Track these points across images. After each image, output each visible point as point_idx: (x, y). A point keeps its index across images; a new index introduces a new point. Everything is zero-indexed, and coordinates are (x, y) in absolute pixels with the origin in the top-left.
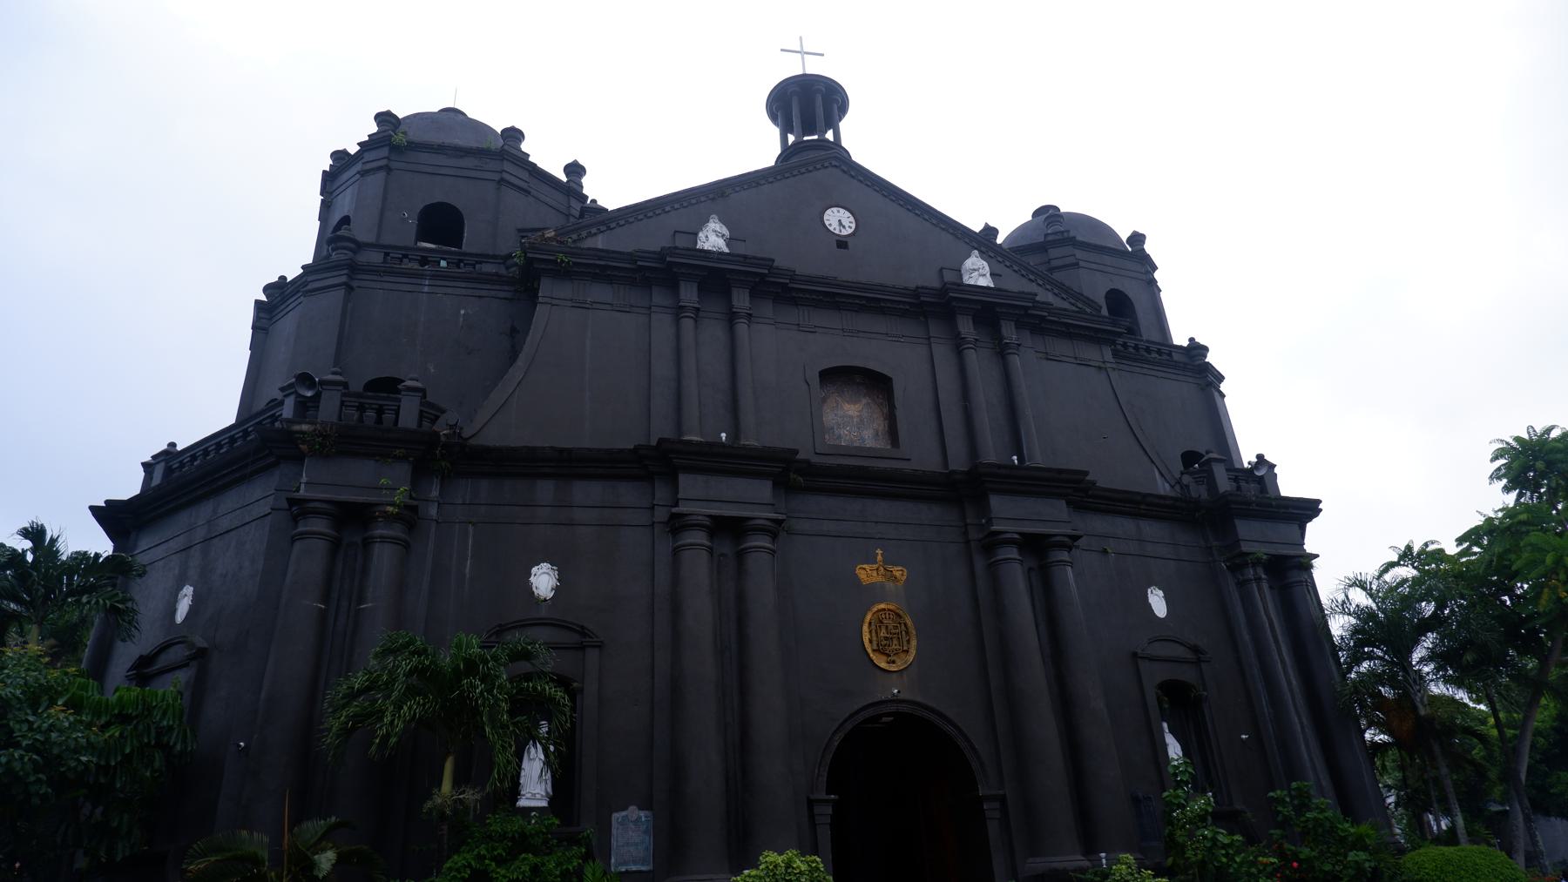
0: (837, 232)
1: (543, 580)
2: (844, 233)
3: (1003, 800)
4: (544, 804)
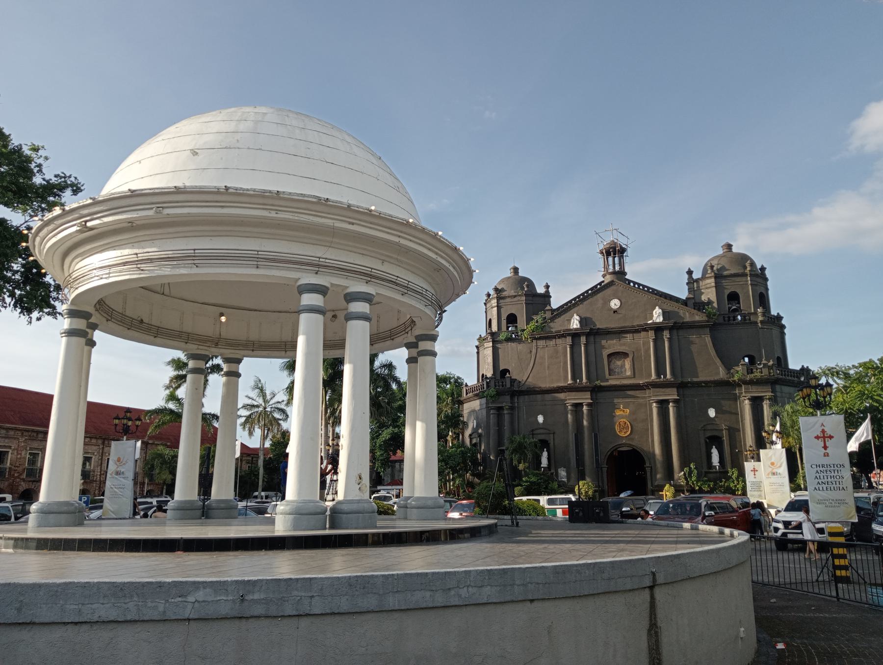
0: (614, 308)
1: (540, 419)
2: (616, 307)
3: (651, 467)
4: (546, 466)
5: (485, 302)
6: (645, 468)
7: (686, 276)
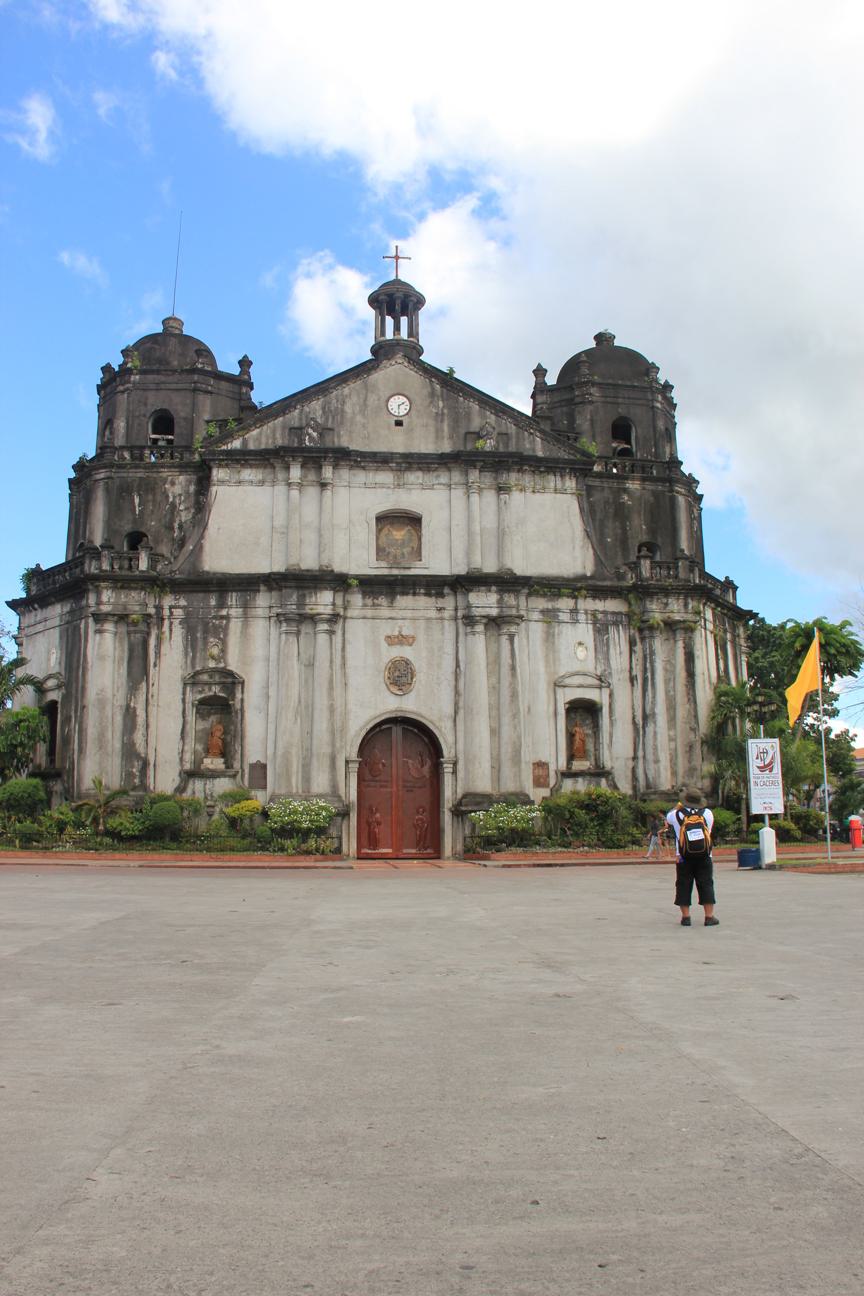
5: (99, 383)
6: (442, 763)
7: (533, 379)
